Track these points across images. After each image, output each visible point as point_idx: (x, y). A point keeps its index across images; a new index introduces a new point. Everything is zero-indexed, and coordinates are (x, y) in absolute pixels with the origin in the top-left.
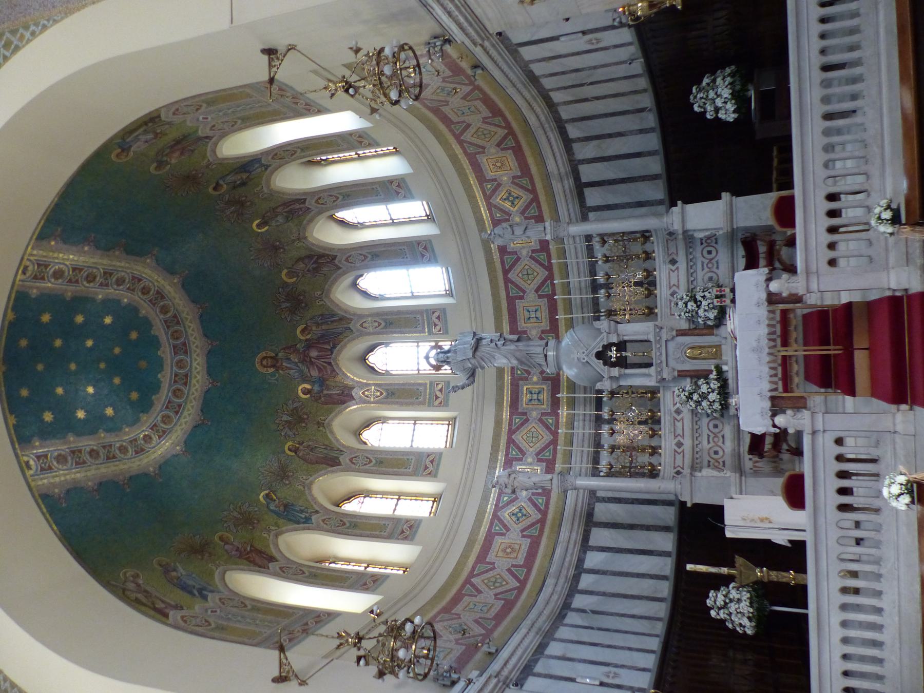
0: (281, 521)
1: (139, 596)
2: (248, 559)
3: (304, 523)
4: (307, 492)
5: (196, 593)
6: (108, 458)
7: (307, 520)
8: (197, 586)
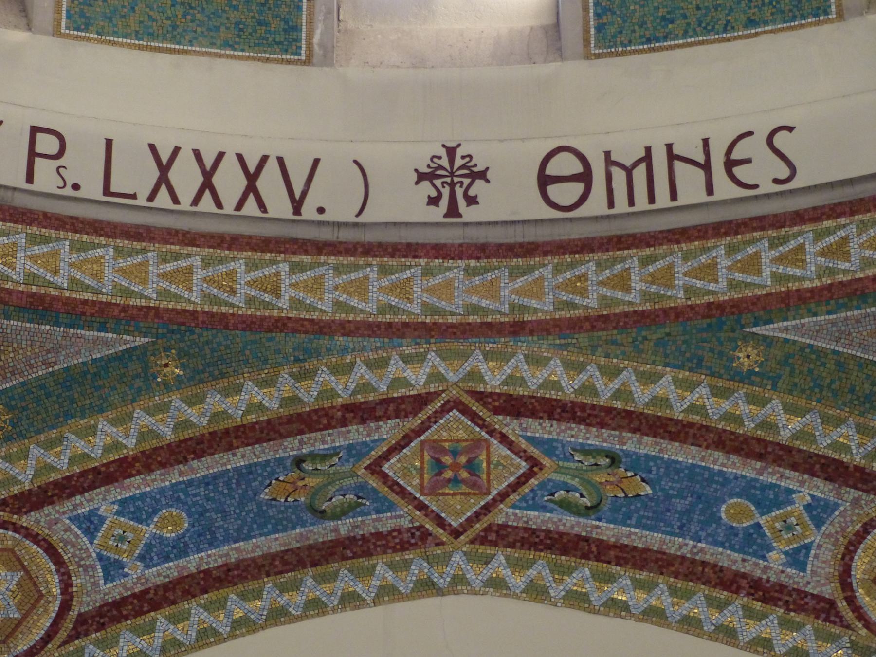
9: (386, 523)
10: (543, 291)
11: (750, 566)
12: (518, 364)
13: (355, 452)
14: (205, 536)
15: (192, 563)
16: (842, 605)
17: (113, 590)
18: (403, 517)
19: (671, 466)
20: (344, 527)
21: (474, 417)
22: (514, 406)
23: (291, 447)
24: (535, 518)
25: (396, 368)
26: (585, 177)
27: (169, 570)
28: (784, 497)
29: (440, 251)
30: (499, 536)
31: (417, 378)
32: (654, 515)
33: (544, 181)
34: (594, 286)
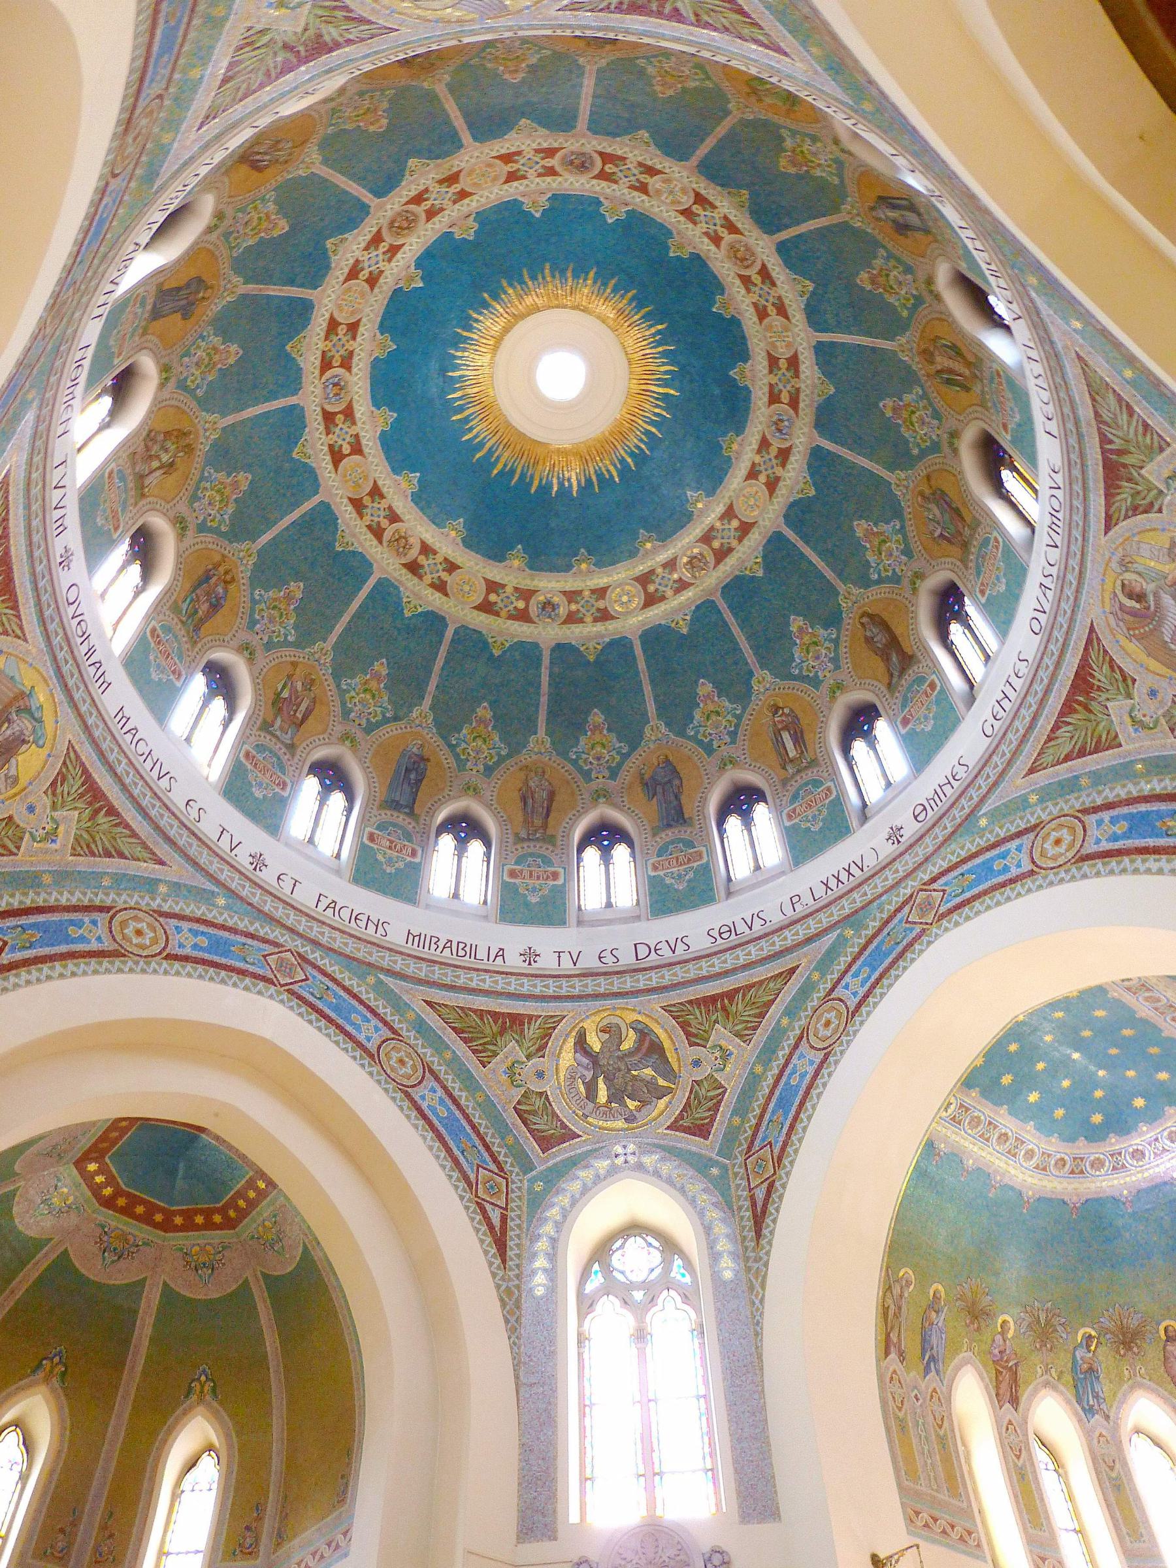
0: (1068, 1378)
1: (892, 1307)
2: (998, 1373)
3: (1083, 1409)
4: (1126, 1386)
5: (927, 1358)
6: (1009, 1152)
7: (1089, 1411)
8: (934, 1352)
9: (914, 934)
10: (929, 844)
11: (1008, 876)
12: (931, 868)
13: (900, 921)
14: (874, 969)
15: (873, 979)
16: (1035, 869)
17: (857, 1000)
18: (918, 928)
19: (978, 866)
20: (904, 943)
21: (925, 890)
22: (934, 880)
23: (885, 931)
24: (949, 905)
25: (902, 891)
26: (925, 809)
27: (868, 985)
28: (1008, 852)
29: (902, 854)
30: (943, 916)
31: (908, 891)
32: (978, 881)
33: (916, 817)
34: (940, 833)
